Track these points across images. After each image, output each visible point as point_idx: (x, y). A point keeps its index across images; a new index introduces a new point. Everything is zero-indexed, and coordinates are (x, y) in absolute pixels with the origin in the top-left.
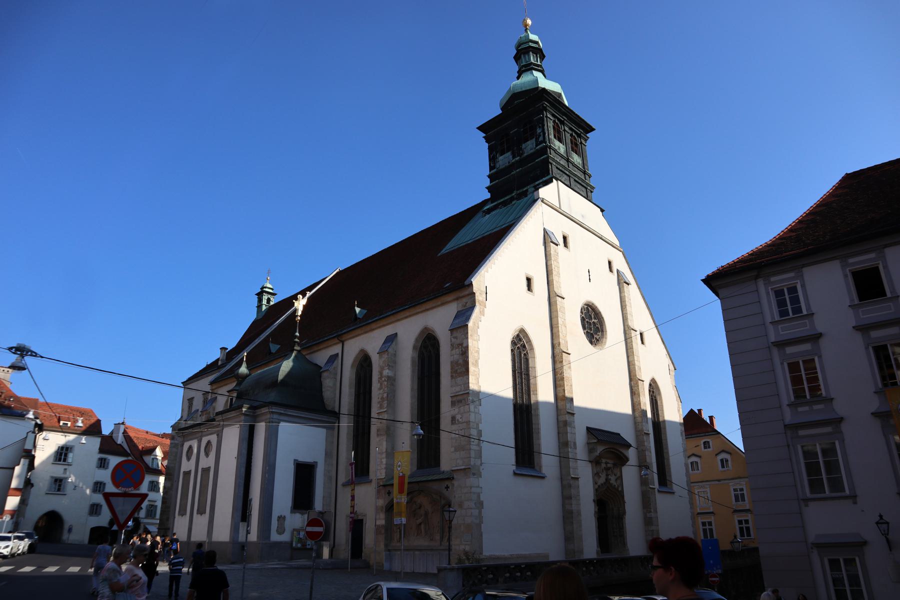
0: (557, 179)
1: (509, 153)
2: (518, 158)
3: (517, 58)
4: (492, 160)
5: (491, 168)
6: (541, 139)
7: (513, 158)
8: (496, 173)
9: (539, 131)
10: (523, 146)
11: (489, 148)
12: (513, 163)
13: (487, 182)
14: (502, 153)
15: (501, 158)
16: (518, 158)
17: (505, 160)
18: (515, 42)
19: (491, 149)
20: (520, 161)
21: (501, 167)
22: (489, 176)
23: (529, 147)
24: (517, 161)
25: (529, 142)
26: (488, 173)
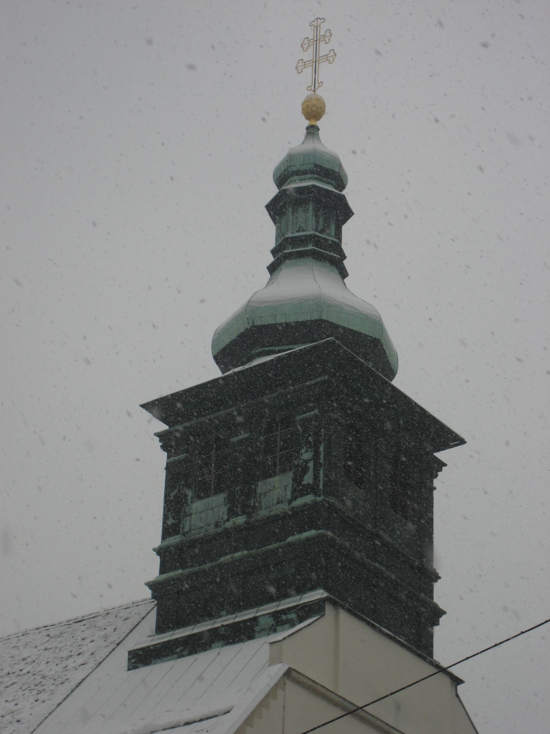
0: (335, 604)
1: (220, 498)
2: (241, 520)
3: (275, 209)
4: (174, 506)
5: (167, 532)
6: (308, 479)
7: (232, 513)
8: (180, 548)
9: (306, 455)
10: (261, 487)
11: (169, 468)
12: (227, 533)
13: (152, 569)
14: (203, 492)
15: (197, 505)
16: (241, 520)
17: (208, 512)
18: (276, 158)
19: (175, 477)
20: (249, 526)
21: (196, 534)
22: (159, 551)
23: (275, 493)
24: (238, 529)
25: (276, 480)
26: (157, 542)
